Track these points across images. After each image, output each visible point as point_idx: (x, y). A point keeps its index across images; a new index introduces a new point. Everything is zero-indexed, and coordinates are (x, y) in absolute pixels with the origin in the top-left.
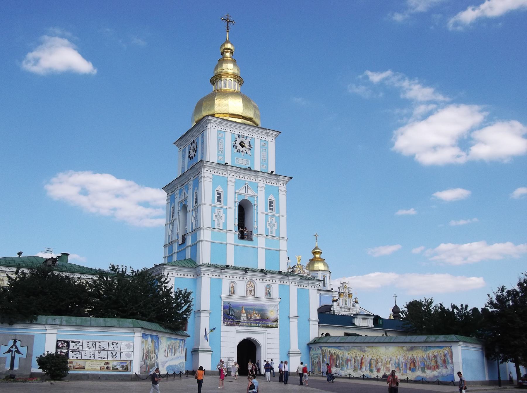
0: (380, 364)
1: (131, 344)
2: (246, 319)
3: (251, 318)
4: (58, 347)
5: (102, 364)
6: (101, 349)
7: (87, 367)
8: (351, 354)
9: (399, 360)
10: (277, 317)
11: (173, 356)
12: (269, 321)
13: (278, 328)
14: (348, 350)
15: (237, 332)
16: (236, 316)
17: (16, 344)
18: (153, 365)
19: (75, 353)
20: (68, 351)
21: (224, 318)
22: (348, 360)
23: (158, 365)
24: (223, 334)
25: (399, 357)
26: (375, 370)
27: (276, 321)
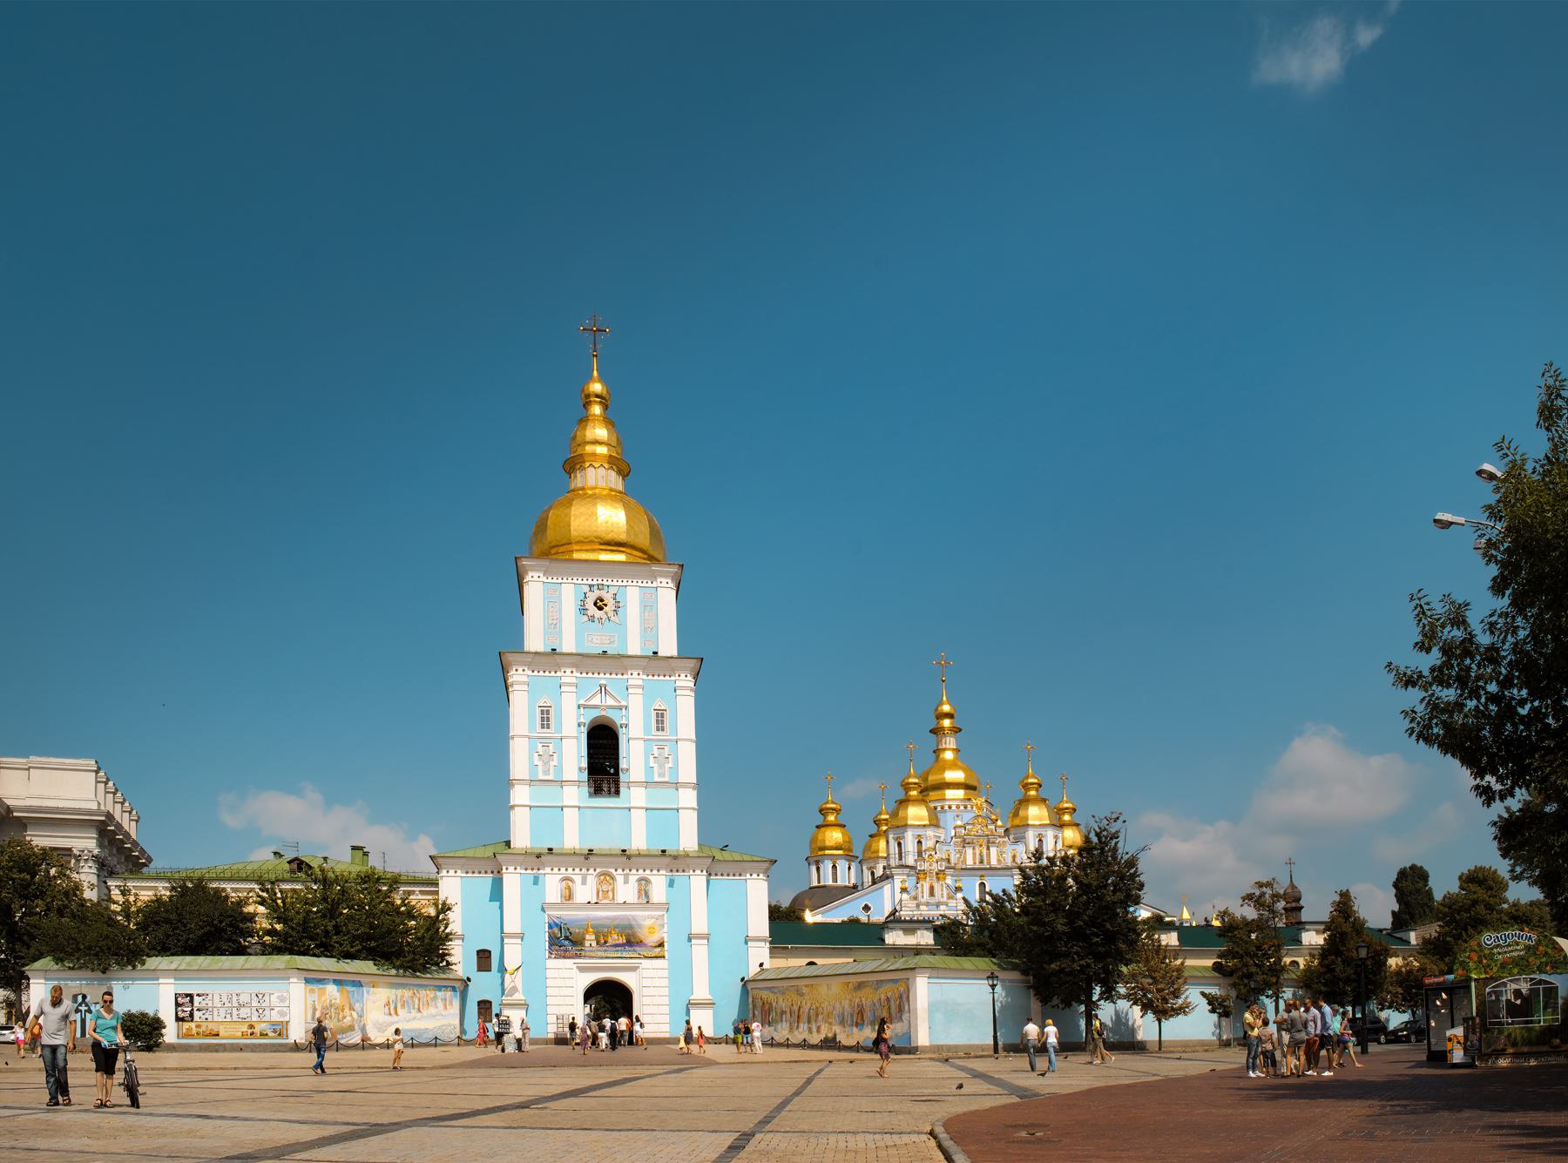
0: (820, 1017)
1: (285, 995)
2: (594, 944)
3: (606, 942)
4: (177, 1005)
5: (245, 1028)
6: (241, 1006)
7: (222, 1033)
8: (786, 1000)
9: (843, 1008)
10: (663, 938)
11: (419, 1015)
12: (645, 945)
13: (664, 957)
14: (784, 993)
15: (582, 969)
16: (574, 940)
17: (87, 1000)
18: (351, 1028)
19: (204, 1012)
20: (192, 1010)
21: (551, 945)
22: (783, 1012)
23: (363, 1029)
24: (549, 973)
25: (843, 1002)
26: (814, 1030)
27: (661, 945)
